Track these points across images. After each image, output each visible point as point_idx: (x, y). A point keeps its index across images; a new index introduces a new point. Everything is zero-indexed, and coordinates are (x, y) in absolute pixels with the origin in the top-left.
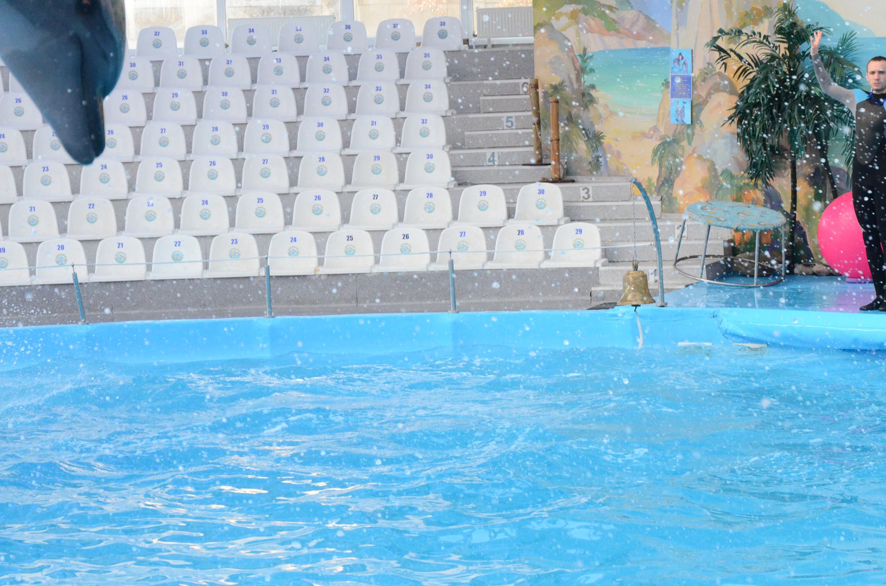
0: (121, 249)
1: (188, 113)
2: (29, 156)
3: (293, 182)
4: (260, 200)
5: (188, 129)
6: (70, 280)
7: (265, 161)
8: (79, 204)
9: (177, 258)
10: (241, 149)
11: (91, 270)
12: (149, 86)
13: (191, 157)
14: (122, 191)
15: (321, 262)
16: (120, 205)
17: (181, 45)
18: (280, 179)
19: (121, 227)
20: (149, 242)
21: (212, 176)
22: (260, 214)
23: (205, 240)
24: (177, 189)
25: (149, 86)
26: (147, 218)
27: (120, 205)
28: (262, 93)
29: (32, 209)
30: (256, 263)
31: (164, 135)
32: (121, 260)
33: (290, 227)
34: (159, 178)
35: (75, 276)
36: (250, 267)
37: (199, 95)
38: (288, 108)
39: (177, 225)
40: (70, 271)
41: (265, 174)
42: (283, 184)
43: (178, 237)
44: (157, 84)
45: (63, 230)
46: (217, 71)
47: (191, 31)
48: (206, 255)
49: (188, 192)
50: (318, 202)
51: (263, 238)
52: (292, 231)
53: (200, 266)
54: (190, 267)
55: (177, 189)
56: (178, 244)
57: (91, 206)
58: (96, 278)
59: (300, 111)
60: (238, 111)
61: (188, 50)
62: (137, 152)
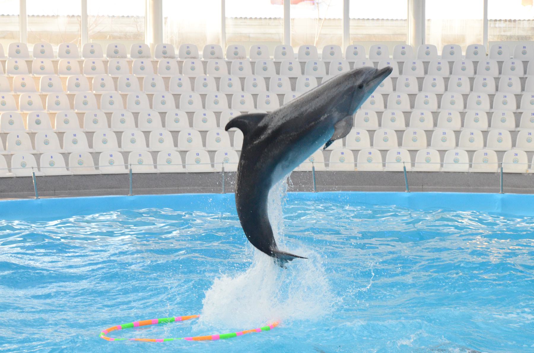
1: (466, 88)
2: (386, 107)
3: (517, 125)
4: (500, 134)
6: (402, 170)
7: (503, 114)
8: (409, 132)
9: (456, 161)
10: (491, 107)
11: (413, 165)
12: (447, 74)
13: (466, 110)
14: (430, 127)
15: (529, 167)
16: (429, 133)
17: (464, 53)
18: (511, 123)
19: (429, 145)
20: (442, 152)
21: (476, 120)
22: (500, 141)
23: (471, 153)
24: (458, 127)
25: (447, 74)
26: (442, 140)
27: (429, 133)
28: (504, 80)
29: (386, 133)
30: (496, 165)
31: (453, 99)
32: (428, 161)
33: (514, 148)
34: (449, 120)
35: (405, 168)
36: (493, 168)
37: (472, 79)
38: (517, 88)
39: (457, 145)
40: (402, 165)
41: (503, 121)
42: (513, 126)
43: (458, 150)
44: (451, 73)
45: (400, 144)
46: (481, 67)
47: (469, 47)
48: (471, 160)
49: (463, 128)
50: (530, 136)
51: (500, 153)
52: (515, 150)
54: (463, 167)
55: (458, 127)
56: (457, 154)
57: (415, 133)
58: (415, 169)
59: (523, 89)
60: (491, 88)
61: (467, 56)
62: (439, 107)
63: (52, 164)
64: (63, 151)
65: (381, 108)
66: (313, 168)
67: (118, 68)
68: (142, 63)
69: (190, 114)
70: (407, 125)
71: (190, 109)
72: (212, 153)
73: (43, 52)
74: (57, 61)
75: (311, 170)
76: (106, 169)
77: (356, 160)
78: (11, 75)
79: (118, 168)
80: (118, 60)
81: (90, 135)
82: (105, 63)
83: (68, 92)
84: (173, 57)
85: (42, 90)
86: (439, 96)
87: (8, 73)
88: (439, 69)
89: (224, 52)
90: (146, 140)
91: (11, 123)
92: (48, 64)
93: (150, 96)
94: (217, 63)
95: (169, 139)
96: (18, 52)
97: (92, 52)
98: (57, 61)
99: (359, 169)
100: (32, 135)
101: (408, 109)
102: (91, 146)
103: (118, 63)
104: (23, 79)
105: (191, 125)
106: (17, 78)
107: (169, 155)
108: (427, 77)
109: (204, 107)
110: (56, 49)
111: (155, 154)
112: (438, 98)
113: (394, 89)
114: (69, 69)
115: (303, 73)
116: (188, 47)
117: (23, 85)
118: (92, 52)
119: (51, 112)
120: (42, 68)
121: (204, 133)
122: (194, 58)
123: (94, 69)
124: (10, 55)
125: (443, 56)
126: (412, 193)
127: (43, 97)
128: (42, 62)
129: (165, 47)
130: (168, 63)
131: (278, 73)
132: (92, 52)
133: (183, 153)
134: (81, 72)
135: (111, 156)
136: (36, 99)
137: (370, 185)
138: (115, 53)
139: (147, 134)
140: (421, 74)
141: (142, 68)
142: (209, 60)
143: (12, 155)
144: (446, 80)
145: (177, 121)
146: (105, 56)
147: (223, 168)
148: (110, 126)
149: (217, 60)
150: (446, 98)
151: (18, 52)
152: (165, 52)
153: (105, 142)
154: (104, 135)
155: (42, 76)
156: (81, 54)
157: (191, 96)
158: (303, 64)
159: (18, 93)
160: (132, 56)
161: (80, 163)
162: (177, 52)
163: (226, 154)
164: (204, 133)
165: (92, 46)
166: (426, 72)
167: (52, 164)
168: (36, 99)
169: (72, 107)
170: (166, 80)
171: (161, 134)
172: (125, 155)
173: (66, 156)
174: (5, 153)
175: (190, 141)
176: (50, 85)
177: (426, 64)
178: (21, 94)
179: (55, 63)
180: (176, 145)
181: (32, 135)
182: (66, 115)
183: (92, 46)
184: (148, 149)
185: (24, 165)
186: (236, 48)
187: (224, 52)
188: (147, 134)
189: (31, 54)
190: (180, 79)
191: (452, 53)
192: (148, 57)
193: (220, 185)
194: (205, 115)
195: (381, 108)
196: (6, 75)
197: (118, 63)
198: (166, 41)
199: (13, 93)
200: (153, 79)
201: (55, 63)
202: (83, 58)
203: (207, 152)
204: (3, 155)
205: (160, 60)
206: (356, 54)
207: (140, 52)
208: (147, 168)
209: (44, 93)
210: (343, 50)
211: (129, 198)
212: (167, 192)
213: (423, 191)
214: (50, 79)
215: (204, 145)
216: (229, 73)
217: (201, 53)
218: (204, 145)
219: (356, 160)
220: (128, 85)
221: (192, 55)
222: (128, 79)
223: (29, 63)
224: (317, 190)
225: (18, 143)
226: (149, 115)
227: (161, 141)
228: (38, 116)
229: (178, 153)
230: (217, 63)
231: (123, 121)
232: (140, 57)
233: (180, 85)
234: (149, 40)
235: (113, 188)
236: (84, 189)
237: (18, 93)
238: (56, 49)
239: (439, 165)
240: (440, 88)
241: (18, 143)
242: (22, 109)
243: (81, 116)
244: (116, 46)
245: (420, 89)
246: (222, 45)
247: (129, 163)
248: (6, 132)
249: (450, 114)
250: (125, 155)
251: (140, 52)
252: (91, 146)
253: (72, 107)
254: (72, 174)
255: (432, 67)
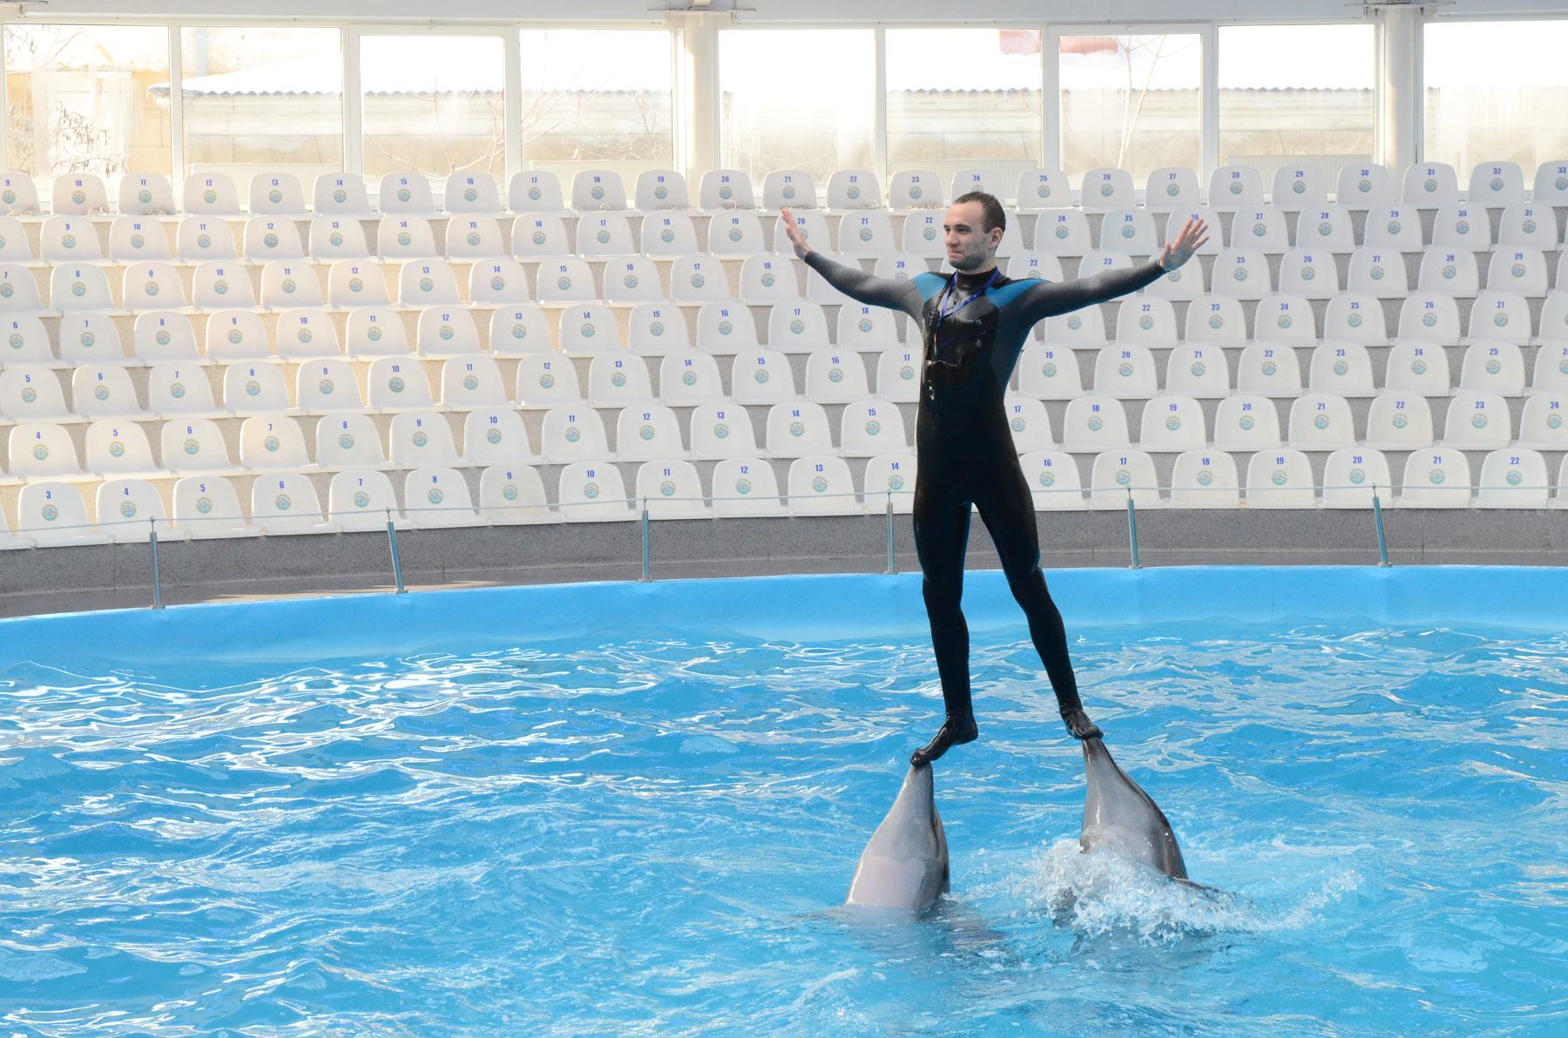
0: (1438, 466)
2: (1319, 333)
5: (1535, 303)
6: (1370, 505)
8: (1386, 397)
9: (1513, 480)
11: (1397, 491)
12: (1484, 242)
14: (1441, 386)
16: (1438, 404)
17: (1529, 185)
19: (1438, 435)
20: (1476, 457)
24: (1517, 386)
25: (1484, 242)
27: (1438, 404)
29: (1321, 406)
32: (1437, 478)
34: (1493, 369)
35: (1376, 500)
39: (1515, 436)
40: (1370, 494)
44: (1494, 240)
45: (1360, 435)
47: (1544, 168)
53: (1545, 493)
55: (1517, 386)
56: (1515, 461)
57: (1400, 405)
58: (1403, 502)
62: (1464, 332)
63: (435, 497)
64: (463, 462)
65: (1309, 338)
66: (1131, 502)
67: (604, 238)
68: (667, 222)
69: (798, 360)
70: (1379, 382)
71: (797, 344)
72: (857, 463)
73: (404, 197)
74: (444, 222)
75: (1124, 506)
76: (576, 508)
77: (1242, 481)
78: (324, 261)
79: (609, 507)
80: (603, 214)
81: (532, 418)
82: (571, 223)
83: (474, 305)
84: (749, 207)
85: (403, 299)
86: (1465, 303)
87: (317, 254)
88: (1462, 229)
89: (884, 190)
90: (682, 430)
91: (326, 388)
92: (420, 230)
93: (690, 312)
94: (865, 220)
95: (741, 425)
96: (340, 198)
97: (535, 195)
98: (444, 222)
99: (1252, 503)
100: (382, 421)
101: (1380, 338)
102: (536, 448)
103: (603, 223)
104: (355, 270)
105: (800, 388)
106: (339, 270)
107: (744, 470)
108: (1429, 250)
109: (833, 340)
110: (438, 187)
111: (705, 467)
112: (1460, 307)
113: (1343, 286)
114: (474, 241)
115: (1095, 244)
116: (788, 179)
117: (356, 287)
118: (535, 195)
119: (430, 357)
120: (405, 240)
121: (834, 410)
122: (805, 207)
123: (539, 240)
124: (319, 208)
125: (1473, 195)
126: (1396, 570)
127: (409, 318)
128: (404, 225)
129: (726, 179)
130: (736, 221)
131: (1028, 245)
132: (533, 192)
133: (782, 464)
134: (507, 251)
135: (591, 474)
136: (392, 328)
137: (1281, 545)
138: (596, 194)
139: (684, 413)
140: (1415, 244)
141: (668, 237)
142: (844, 213)
143: (332, 474)
144: (1483, 258)
145: (762, 378)
146: (568, 204)
147: (890, 507)
148: (584, 395)
149: (864, 213)
150: (1484, 308)
151: (340, 198)
152: (726, 192)
153: (573, 436)
154: (572, 418)
155: (404, 262)
156: (504, 200)
157: (797, 312)
158: (1095, 220)
159: (343, 309)
160: (639, 205)
161: (510, 494)
162: (758, 191)
163: (896, 466)
164: (834, 410)
165: (534, 180)
166: (1427, 239)
167: (435, 497)
168: (392, 328)
169: (484, 344)
170: (732, 267)
171: (721, 415)
172: (629, 470)
173: (472, 475)
174: (313, 468)
175: (797, 431)
176: (427, 286)
177: (1427, 215)
178: (352, 310)
179: (438, 225)
180: (761, 443)
181: (382, 421)
182: (470, 367)
183: (534, 180)
184: (686, 455)
185: (361, 501)
186: (916, 179)
187: (884, 190)
188: (684, 413)
189: (375, 202)
190: (768, 266)
191: (1496, 186)
192: (682, 206)
193: (883, 549)
194: (836, 360)
195: (1309, 338)
196: (309, 260)
197: (603, 223)
198: (727, 163)
199: (328, 308)
200: (697, 266)
201: (438, 225)
202: (510, 213)
203: (843, 462)
204: (308, 475)
205: (713, 214)
206: (1236, 190)
207: (661, 192)
208: (685, 505)
209: (411, 308)
210: (1203, 180)
211: (643, 587)
212: (740, 570)
213: (1423, 562)
214: (426, 270)
215: (836, 442)
216: (898, 247)
217: (822, 193)
218: (836, 442)
219: (1242, 481)
220: (631, 283)
221: (796, 200)
222: (630, 267)
223: (370, 226)
224: (1140, 563)
225: (347, 443)
226: (689, 363)
227: (721, 433)
228: (396, 369)
229: (767, 466)
230: (865, 220)
231: (619, 381)
232: (662, 208)
233: (768, 282)
234: (684, 160)
235: (595, 560)
236: (523, 563)
237: (343, 309)
238: (438, 187)
239: (1468, 492)
240: (1466, 281)
241: (347, 443)
242: (354, 351)
243: (508, 366)
244: (597, 179)
245: (1413, 285)
246: (879, 172)
247: (638, 495)
248: (313, 412)
249: (1494, 351)
250: (629, 470)
251: (661, 194)
252: (536, 448)
253: (484, 344)
254: (490, 523)
255: (1444, 225)
